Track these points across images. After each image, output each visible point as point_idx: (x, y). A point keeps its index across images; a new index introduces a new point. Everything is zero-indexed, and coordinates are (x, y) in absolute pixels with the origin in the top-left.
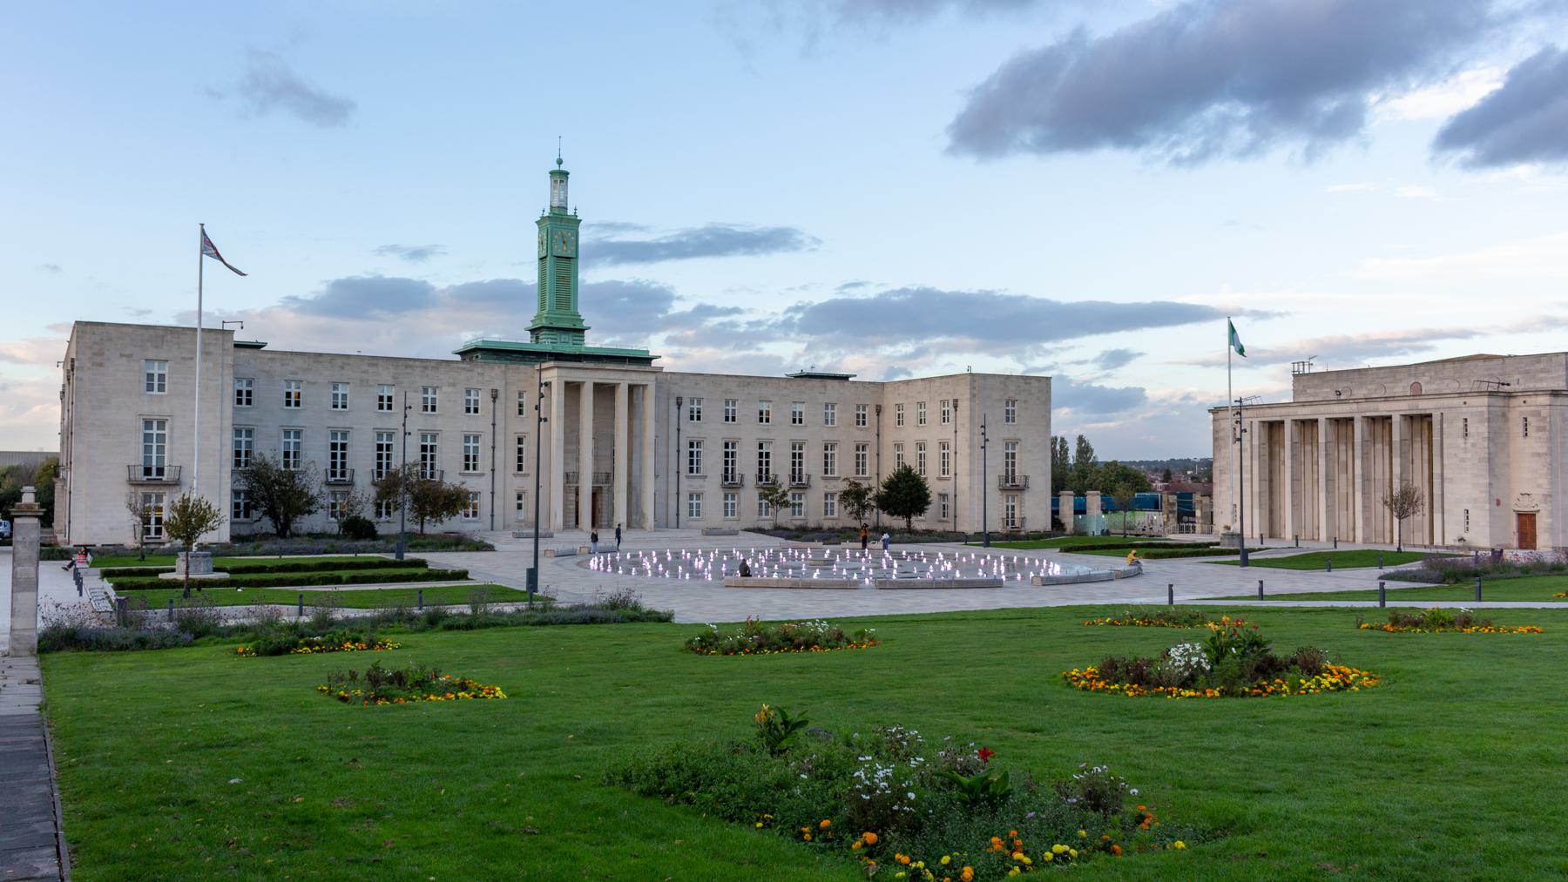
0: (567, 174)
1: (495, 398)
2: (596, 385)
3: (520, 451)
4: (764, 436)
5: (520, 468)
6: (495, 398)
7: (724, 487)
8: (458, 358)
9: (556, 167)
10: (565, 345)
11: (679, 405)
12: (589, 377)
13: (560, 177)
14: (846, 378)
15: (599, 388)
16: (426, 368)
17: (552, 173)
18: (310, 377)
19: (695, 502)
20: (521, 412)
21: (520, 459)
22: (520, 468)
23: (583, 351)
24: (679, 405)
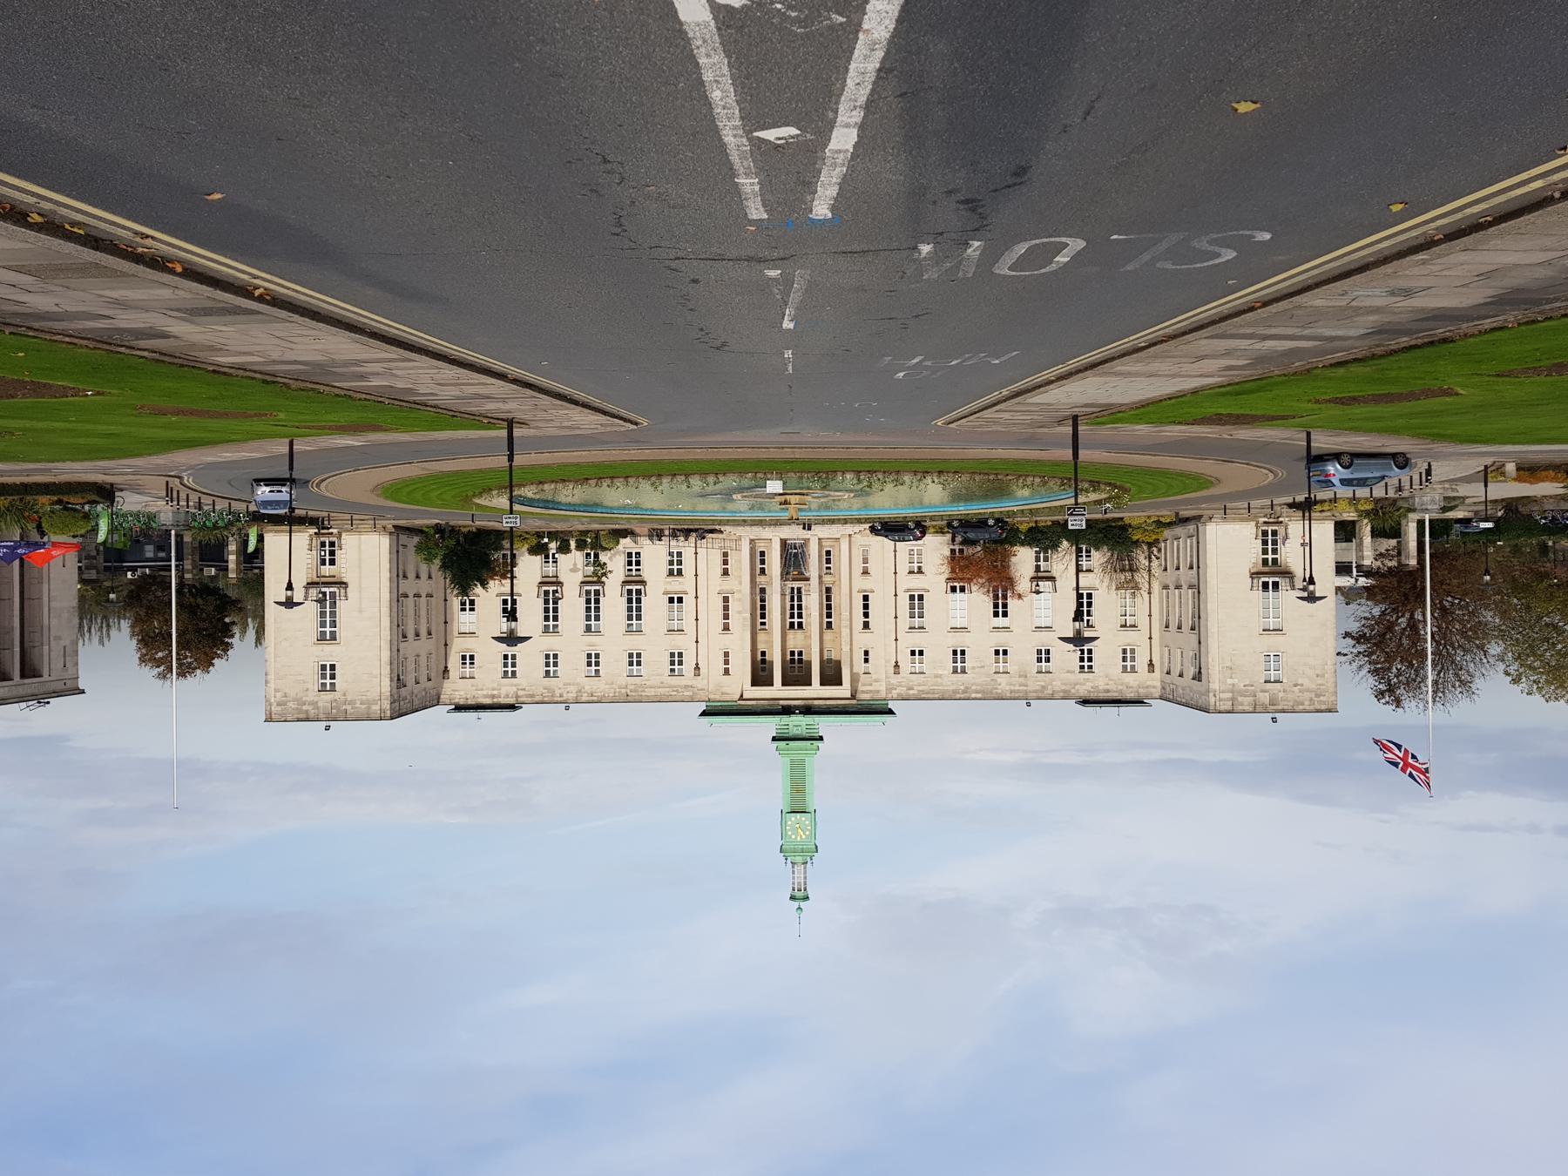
0: (793, 898)
1: (897, 665)
3: (866, 615)
4: (592, 638)
5: (866, 598)
6: (897, 665)
7: (643, 583)
8: (891, 705)
9: (803, 904)
10: (797, 723)
11: (697, 668)
12: (777, 691)
14: (459, 708)
17: (807, 898)
19: (675, 567)
20: (866, 653)
21: (866, 607)
22: (866, 598)
24: (697, 668)
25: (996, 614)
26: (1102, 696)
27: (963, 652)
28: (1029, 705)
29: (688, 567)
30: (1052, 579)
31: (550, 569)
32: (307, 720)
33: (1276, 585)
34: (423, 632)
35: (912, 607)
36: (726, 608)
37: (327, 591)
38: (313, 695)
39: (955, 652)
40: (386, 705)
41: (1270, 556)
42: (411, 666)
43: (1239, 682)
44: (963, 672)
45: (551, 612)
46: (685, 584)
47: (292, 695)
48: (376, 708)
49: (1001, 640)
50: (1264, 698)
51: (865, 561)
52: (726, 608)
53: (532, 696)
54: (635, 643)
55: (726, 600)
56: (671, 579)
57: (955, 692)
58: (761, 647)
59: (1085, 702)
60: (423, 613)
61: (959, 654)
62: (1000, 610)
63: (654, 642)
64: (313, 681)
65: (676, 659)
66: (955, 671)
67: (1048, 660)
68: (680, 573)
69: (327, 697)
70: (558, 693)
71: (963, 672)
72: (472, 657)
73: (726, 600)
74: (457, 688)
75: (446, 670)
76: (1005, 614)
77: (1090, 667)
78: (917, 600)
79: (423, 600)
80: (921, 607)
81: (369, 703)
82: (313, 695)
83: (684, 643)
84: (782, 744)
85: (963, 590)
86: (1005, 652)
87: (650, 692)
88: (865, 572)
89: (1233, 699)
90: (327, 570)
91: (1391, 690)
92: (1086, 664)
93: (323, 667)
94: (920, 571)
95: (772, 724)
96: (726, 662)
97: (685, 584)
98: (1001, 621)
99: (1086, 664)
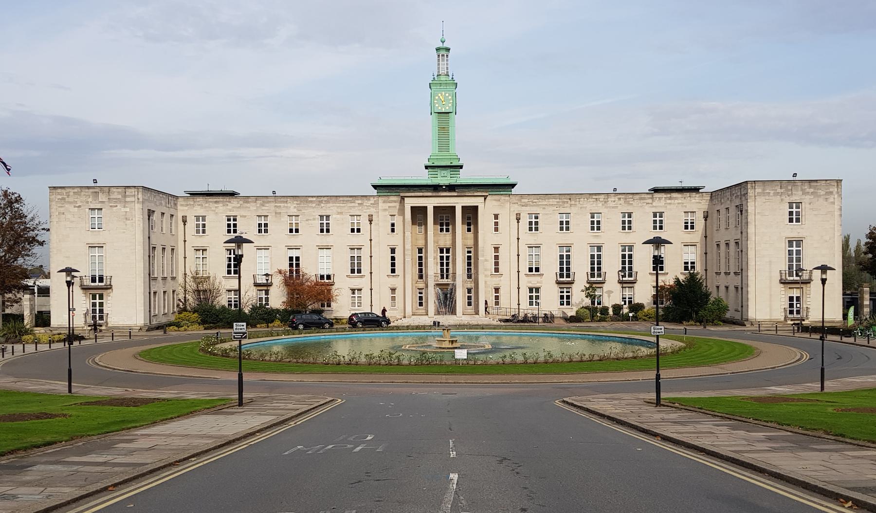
1: (371, 221)
2: (412, 208)
3: (393, 258)
5: (393, 271)
6: (371, 221)
7: (558, 283)
9: (440, 45)
10: (443, 178)
11: (518, 220)
12: (459, 203)
13: (443, 51)
14: (696, 190)
15: (464, 209)
16: (321, 202)
17: (438, 49)
18: (243, 213)
19: (534, 294)
20: (393, 230)
21: (393, 265)
22: (393, 271)
23: (459, 182)
24: (518, 220)
25: (298, 259)
26: (220, 199)
27: (322, 231)
28: (274, 192)
29: (525, 294)
30: (256, 285)
31: (627, 293)
32: (810, 181)
33: (93, 280)
34: (723, 246)
35: (359, 264)
36: (497, 264)
37: (795, 278)
38: (806, 199)
39: (328, 231)
40: (751, 192)
41: (98, 301)
42: (732, 221)
43: (120, 209)
44: (322, 217)
45: (627, 261)
46: (527, 281)
47: (821, 200)
48: (758, 190)
49: (295, 240)
50: (102, 197)
51: (393, 298)
52: (497, 264)
53: (641, 199)
54: (565, 238)
55: (497, 270)
56: (537, 285)
57: (328, 202)
58: (470, 235)
59: (232, 194)
60: (723, 261)
61: (325, 229)
62: (295, 262)
63: (550, 239)
64: (806, 211)
65: (534, 226)
66: (328, 217)
67: (260, 225)
68: (531, 290)
69: (795, 198)
70: (622, 201)
71: (322, 217)
72: (686, 227)
73: (497, 270)
74: (698, 205)
75: (706, 218)
76: (291, 259)
77: (229, 220)
78: (355, 270)
79: (723, 271)
80: (352, 264)
81: (763, 194)
82: (806, 199)
83: (528, 238)
84: (455, 163)
85: (322, 277)
86: (291, 231)
87: (553, 201)
88: (393, 290)
89: (125, 196)
90: (795, 293)
91: (10, 203)
92: (232, 222)
93: (798, 220)
94: (353, 291)
95: (463, 177)
96: (496, 224)
97: (527, 281)
98: (294, 254)
99: (232, 222)
